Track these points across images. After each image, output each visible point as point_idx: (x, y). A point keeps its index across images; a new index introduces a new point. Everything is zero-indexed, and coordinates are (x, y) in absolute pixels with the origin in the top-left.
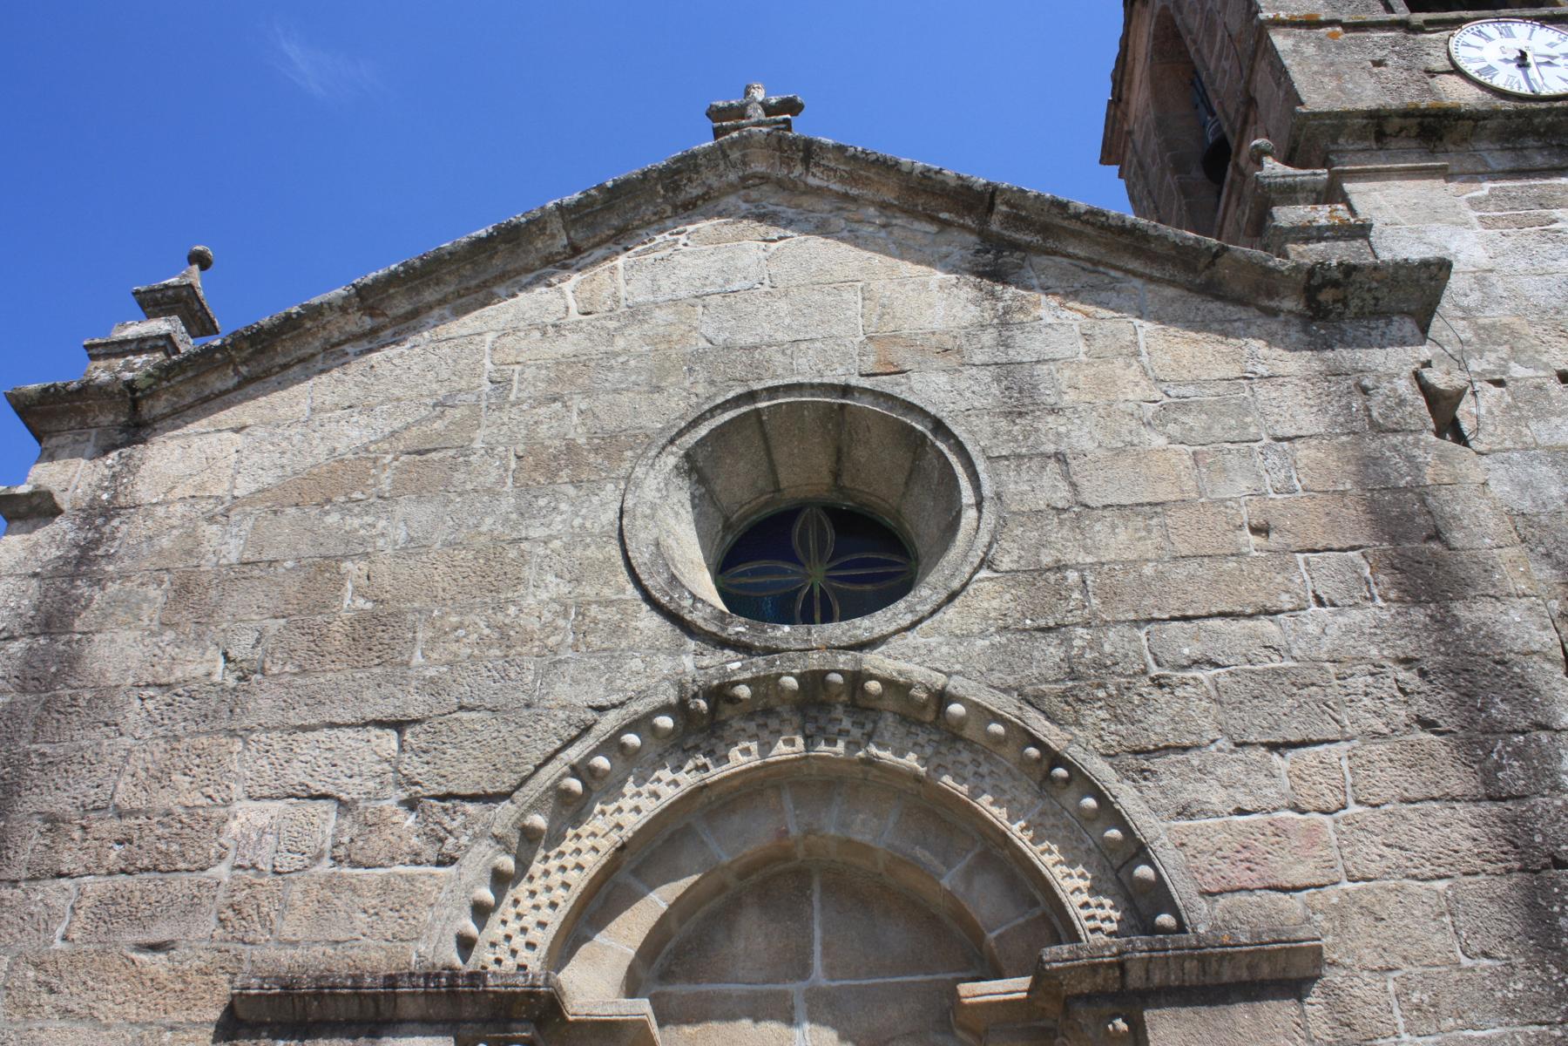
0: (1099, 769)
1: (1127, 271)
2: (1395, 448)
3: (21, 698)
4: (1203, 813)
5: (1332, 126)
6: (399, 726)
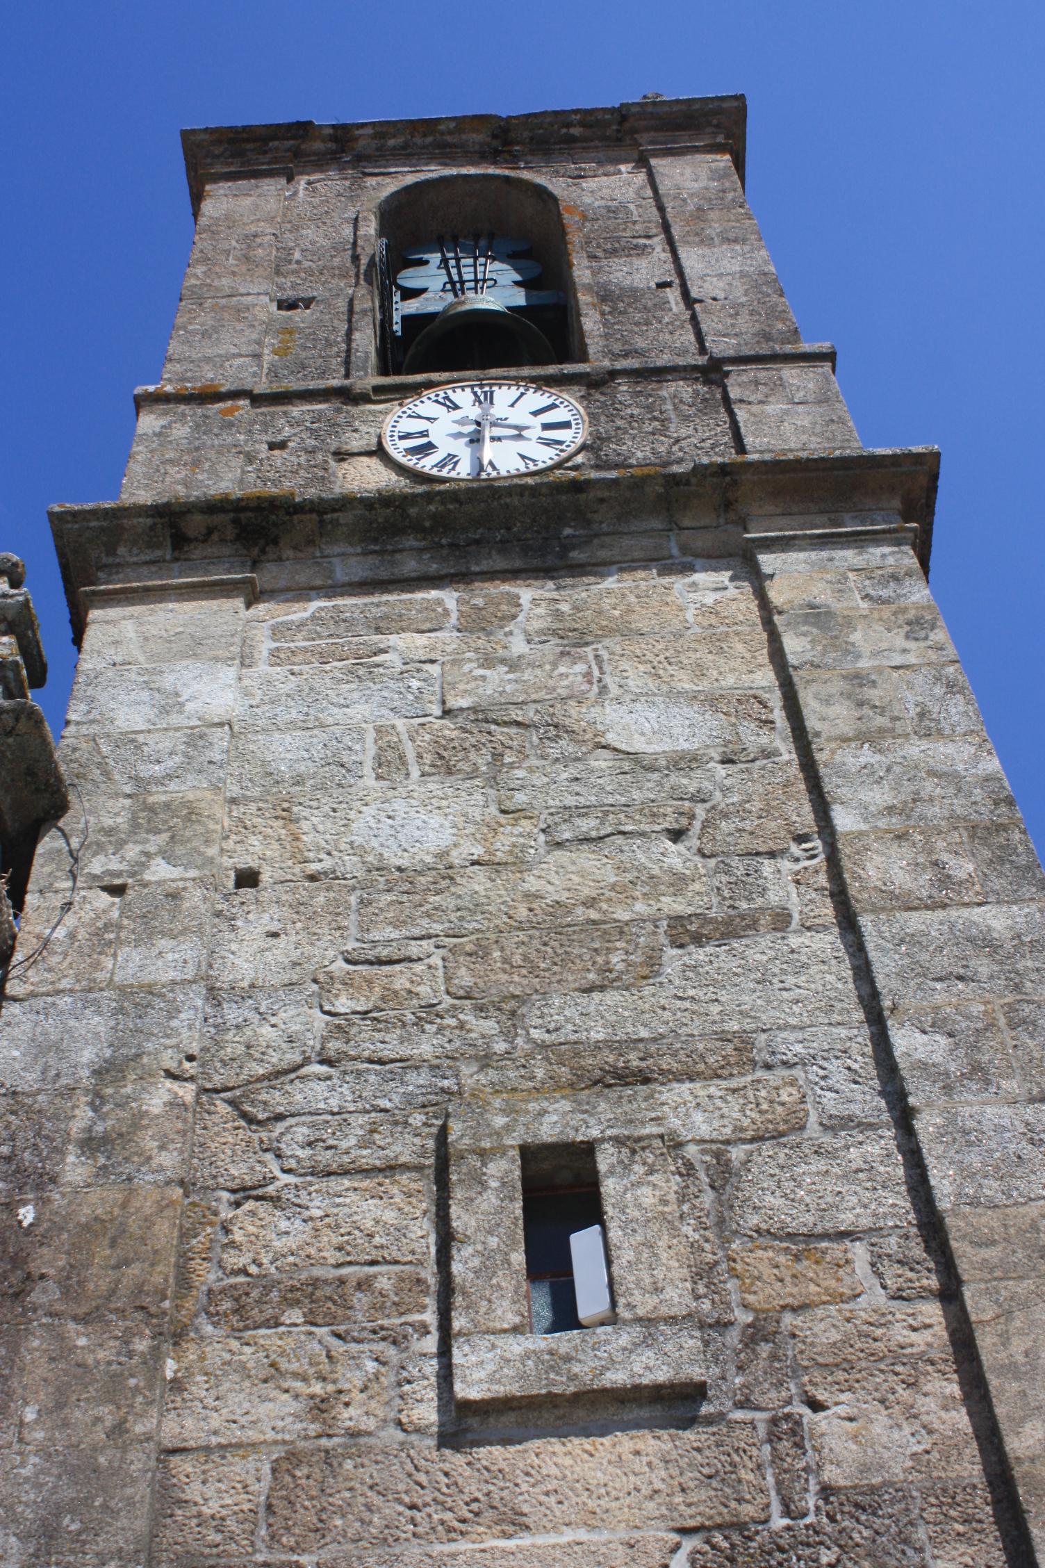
5: (102, 529)
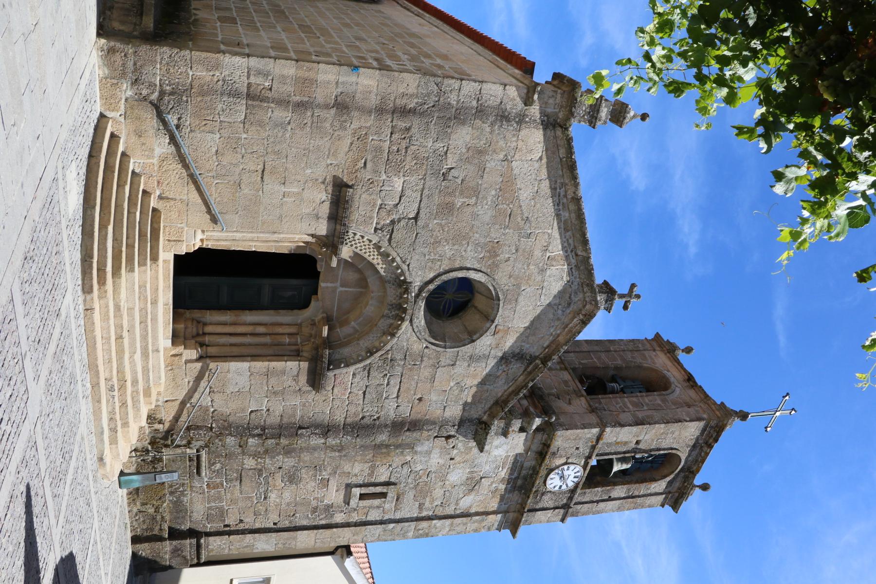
0: (368, 362)
1: (510, 387)
2: (435, 427)
3: (454, 109)
4: (353, 377)
6: (416, 218)
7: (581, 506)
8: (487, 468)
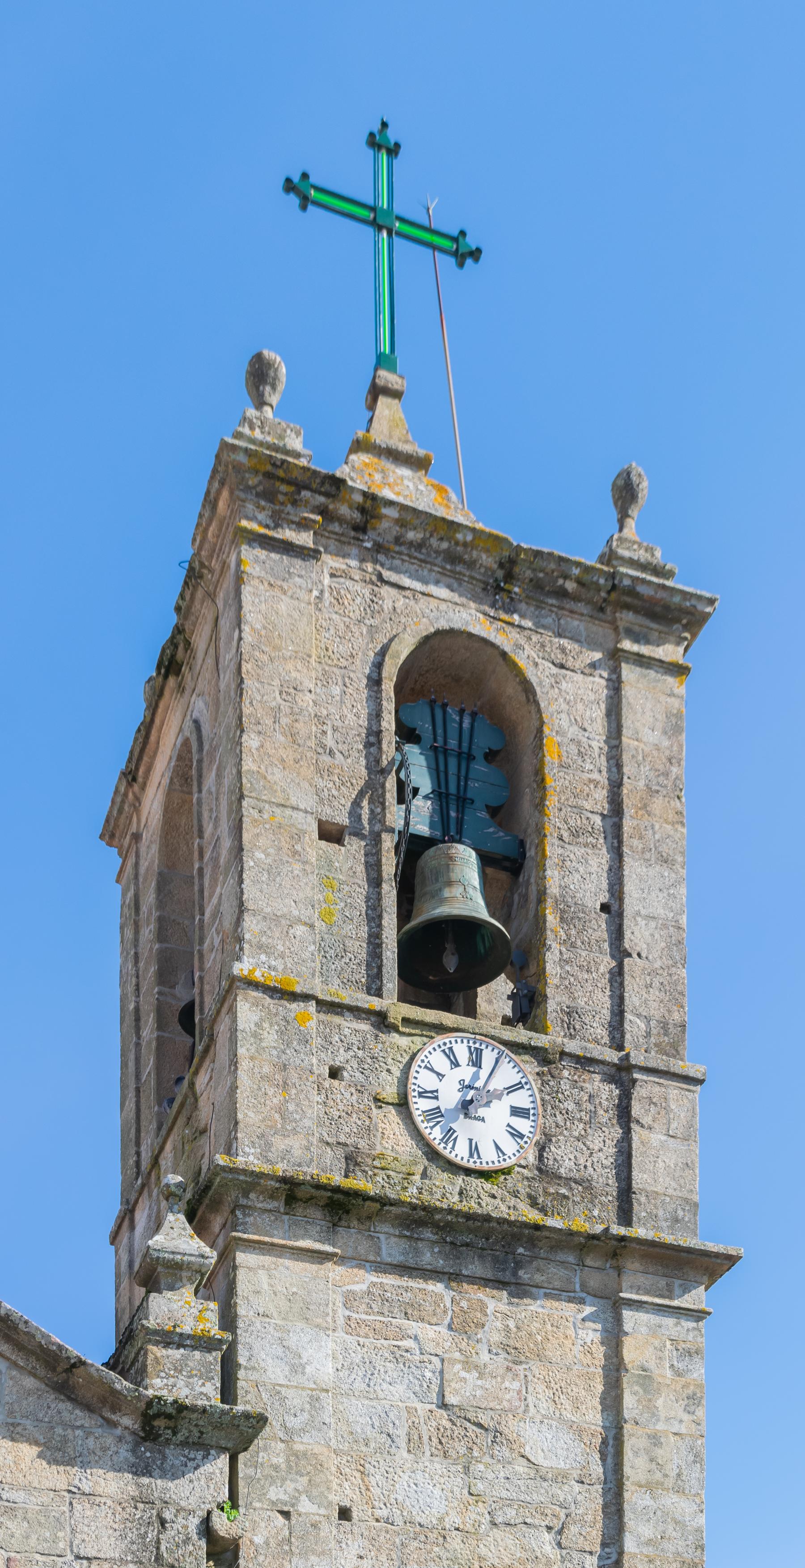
5: (246, 1182)
7: (628, 1016)
8: (399, 1390)
